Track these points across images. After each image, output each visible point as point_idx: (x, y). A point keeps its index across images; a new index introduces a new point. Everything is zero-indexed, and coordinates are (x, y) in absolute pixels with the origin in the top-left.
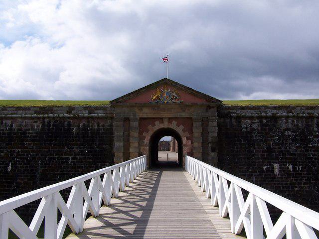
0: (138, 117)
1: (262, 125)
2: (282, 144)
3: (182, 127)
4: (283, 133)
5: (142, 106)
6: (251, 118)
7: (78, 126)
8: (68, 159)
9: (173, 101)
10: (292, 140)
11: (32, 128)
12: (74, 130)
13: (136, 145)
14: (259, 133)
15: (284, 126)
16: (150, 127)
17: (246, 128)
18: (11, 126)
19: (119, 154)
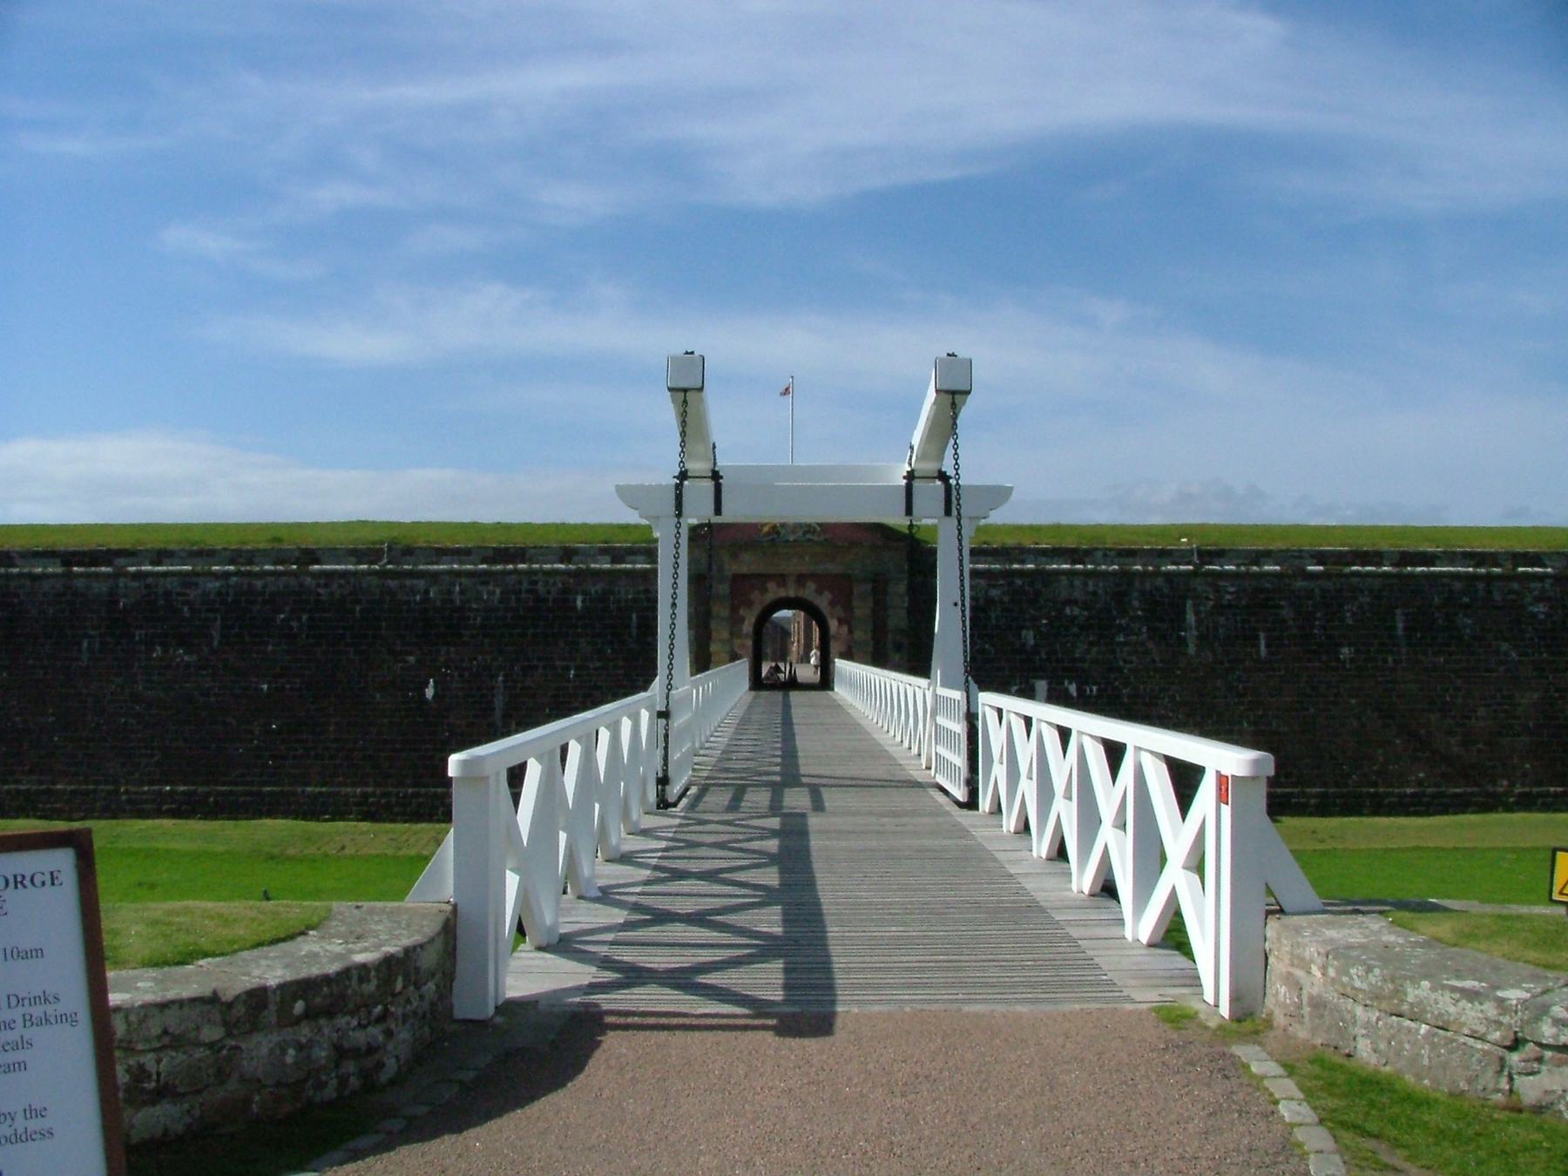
3: (827, 596)
9: (809, 536)
10: (1081, 628)
11: (479, 599)
12: (579, 603)
13: (725, 635)
15: (1064, 594)
16: (755, 595)
18: (427, 592)
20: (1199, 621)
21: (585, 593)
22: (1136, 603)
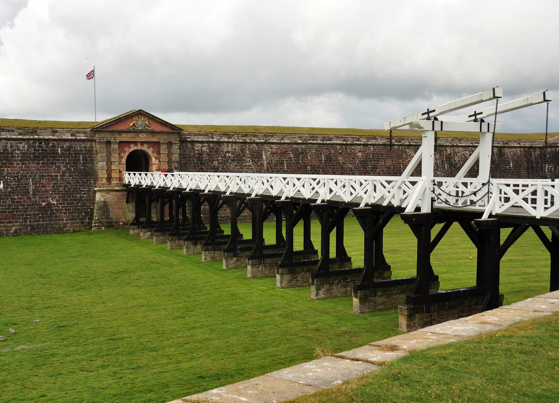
0: (118, 141)
1: (210, 148)
2: (224, 163)
3: (151, 149)
4: (225, 155)
5: (120, 132)
6: (202, 142)
7: (62, 147)
8: (57, 176)
10: (232, 160)
11: (19, 150)
12: (59, 151)
14: (207, 154)
15: (225, 150)
16: (126, 149)
17: (199, 151)
19: (154, 167)
20: (267, 158)
21: (62, 147)
22: (248, 152)
